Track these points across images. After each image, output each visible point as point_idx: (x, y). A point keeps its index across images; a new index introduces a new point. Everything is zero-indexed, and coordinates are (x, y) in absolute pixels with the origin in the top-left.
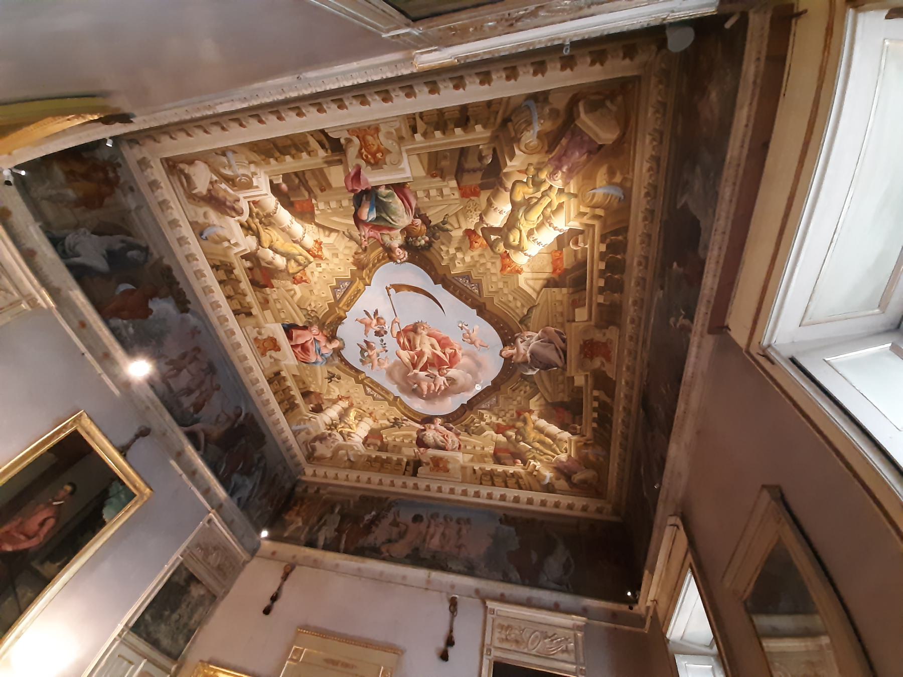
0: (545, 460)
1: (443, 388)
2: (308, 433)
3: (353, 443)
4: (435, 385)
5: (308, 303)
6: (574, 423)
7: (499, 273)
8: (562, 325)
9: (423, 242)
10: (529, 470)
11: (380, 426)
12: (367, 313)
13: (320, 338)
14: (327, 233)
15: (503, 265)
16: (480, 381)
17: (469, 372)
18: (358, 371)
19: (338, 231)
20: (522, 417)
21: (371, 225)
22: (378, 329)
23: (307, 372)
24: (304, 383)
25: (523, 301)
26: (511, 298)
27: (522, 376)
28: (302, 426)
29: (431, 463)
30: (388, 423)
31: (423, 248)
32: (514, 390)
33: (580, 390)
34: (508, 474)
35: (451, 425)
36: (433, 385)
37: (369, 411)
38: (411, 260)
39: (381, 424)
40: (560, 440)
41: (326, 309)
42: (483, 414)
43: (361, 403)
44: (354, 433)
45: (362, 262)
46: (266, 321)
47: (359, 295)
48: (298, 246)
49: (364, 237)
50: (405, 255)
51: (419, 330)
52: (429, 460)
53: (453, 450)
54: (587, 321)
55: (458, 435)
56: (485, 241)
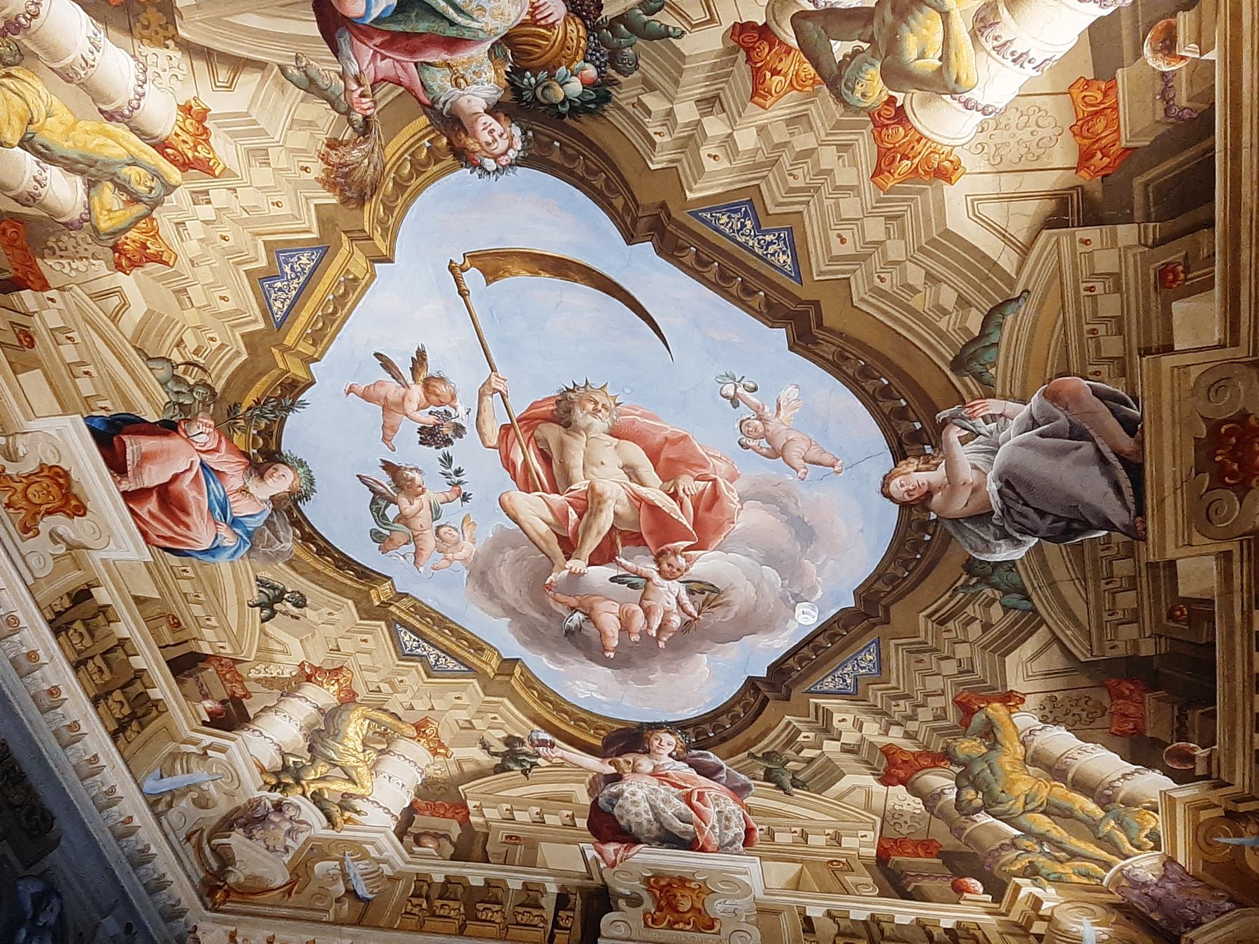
0: (1075, 878)
1: (676, 621)
2: (203, 803)
3: (360, 835)
4: (648, 613)
5: (171, 339)
6: (1183, 737)
7: (868, 187)
8: (1123, 367)
9: (575, 87)
10: (1014, 916)
11: (454, 770)
12: (387, 364)
13: (223, 461)
14: (223, 75)
15: (881, 156)
16: (813, 590)
17: (770, 559)
18: (365, 574)
19: (261, 66)
20: (978, 719)
21: (383, 32)
22: (432, 420)
23: (186, 586)
24: (176, 625)
25: (961, 284)
26: (915, 276)
27: (970, 566)
28: (178, 780)
29: (645, 895)
30: (483, 757)
31: (578, 108)
32: (942, 622)
33: (1200, 610)
34: (936, 933)
35: (713, 758)
36: (641, 614)
37: (415, 718)
38: (533, 159)
39: (459, 763)
40: (1130, 802)
41: (238, 353)
42: (828, 714)
43: (385, 687)
44: (362, 797)
45: (357, 175)
46: (31, 414)
47: (352, 297)
48: (120, 130)
49: (358, 80)
50: (511, 138)
51: (580, 416)
52: (638, 886)
53: (721, 848)
54: (1221, 346)
55: (739, 791)
56: (808, 66)
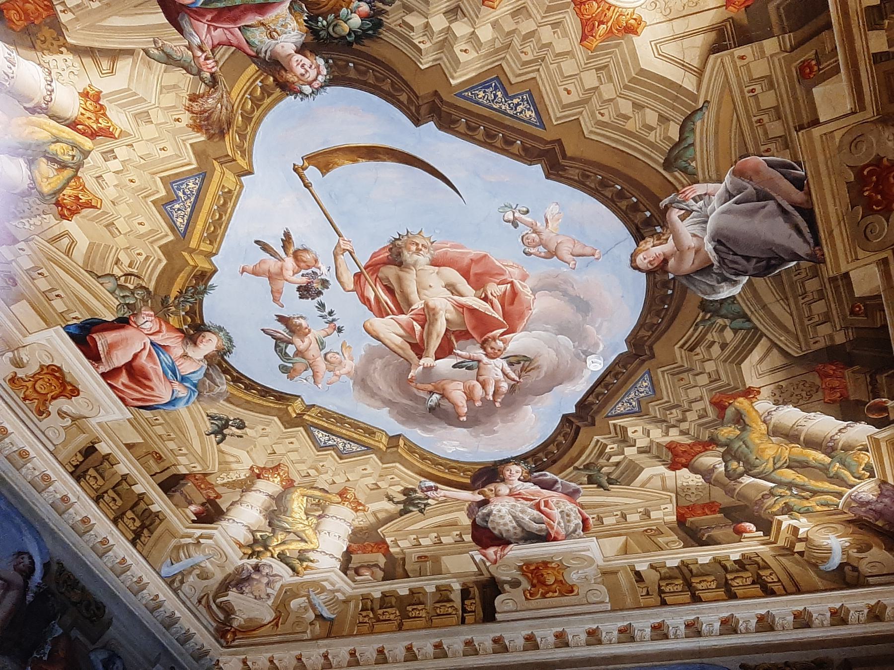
0: (818, 508)
1: (505, 386)
2: (204, 576)
4: (484, 385)
7: (580, 53)
8: (786, 143)
9: (356, 21)
10: (781, 543)
11: (372, 519)
12: (265, 247)
13: (169, 338)
14: (105, 64)
15: (583, 27)
16: (596, 345)
17: (562, 330)
18: (282, 397)
19: (130, 52)
20: (730, 412)
22: (304, 280)
23: (160, 430)
24: (159, 458)
25: (660, 107)
26: (626, 107)
27: (704, 306)
28: (184, 564)
29: (521, 578)
31: (360, 36)
32: (691, 349)
33: (872, 304)
35: (549, 476)
36: (479, 386)
37: (337, 489)
39: (374, 514)
40: (847, 448)
41: (160, 261)
42: (624, 429)
43: (312, 472)
47: (230, 205)
49: (201, 48)
50: (318, 67)
51: (407, 256)
53: (568, 536)
54: (853, 113)
55: (572, 495)
